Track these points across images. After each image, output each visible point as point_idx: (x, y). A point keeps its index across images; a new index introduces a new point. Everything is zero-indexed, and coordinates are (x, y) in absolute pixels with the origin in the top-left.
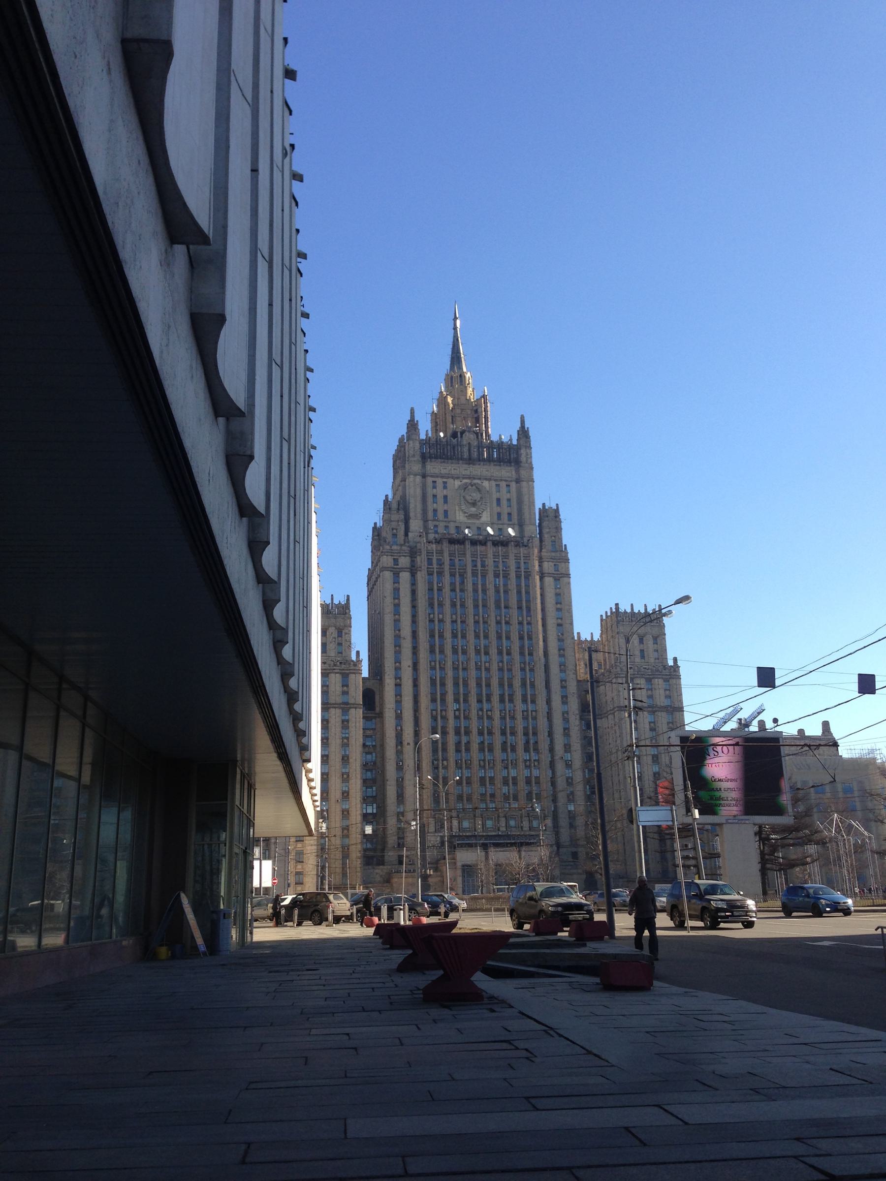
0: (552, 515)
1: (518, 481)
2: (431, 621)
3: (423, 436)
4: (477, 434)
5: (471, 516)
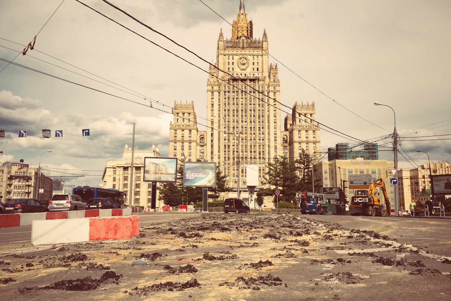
0: (274, 67)
1: (262, 56)
2: (225, 110)
3: (225, 39)
4: (246, 37)
5: (242, 70)
